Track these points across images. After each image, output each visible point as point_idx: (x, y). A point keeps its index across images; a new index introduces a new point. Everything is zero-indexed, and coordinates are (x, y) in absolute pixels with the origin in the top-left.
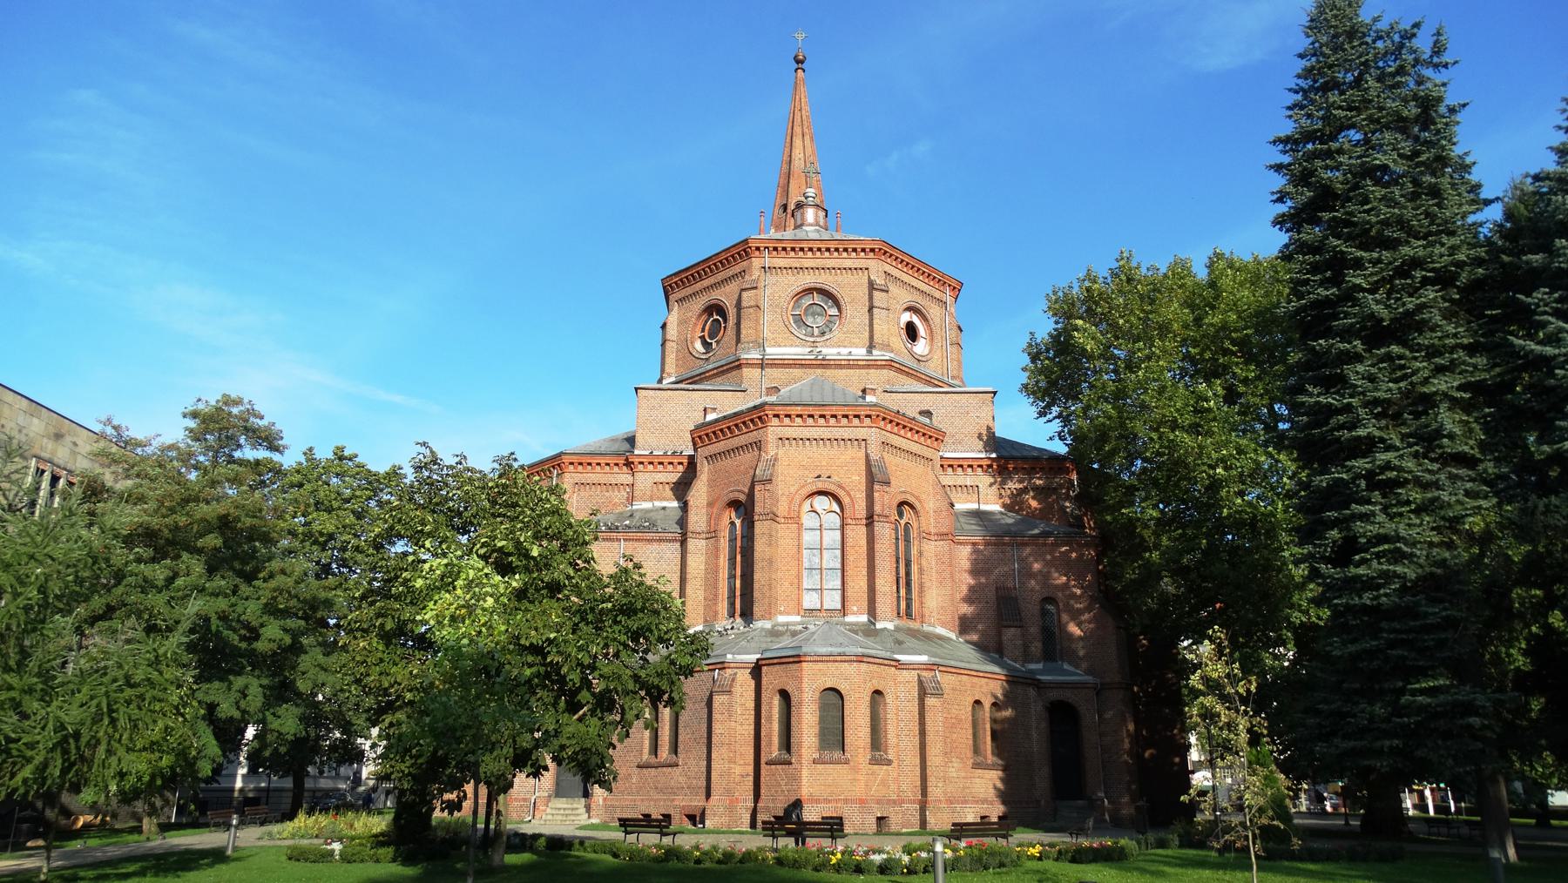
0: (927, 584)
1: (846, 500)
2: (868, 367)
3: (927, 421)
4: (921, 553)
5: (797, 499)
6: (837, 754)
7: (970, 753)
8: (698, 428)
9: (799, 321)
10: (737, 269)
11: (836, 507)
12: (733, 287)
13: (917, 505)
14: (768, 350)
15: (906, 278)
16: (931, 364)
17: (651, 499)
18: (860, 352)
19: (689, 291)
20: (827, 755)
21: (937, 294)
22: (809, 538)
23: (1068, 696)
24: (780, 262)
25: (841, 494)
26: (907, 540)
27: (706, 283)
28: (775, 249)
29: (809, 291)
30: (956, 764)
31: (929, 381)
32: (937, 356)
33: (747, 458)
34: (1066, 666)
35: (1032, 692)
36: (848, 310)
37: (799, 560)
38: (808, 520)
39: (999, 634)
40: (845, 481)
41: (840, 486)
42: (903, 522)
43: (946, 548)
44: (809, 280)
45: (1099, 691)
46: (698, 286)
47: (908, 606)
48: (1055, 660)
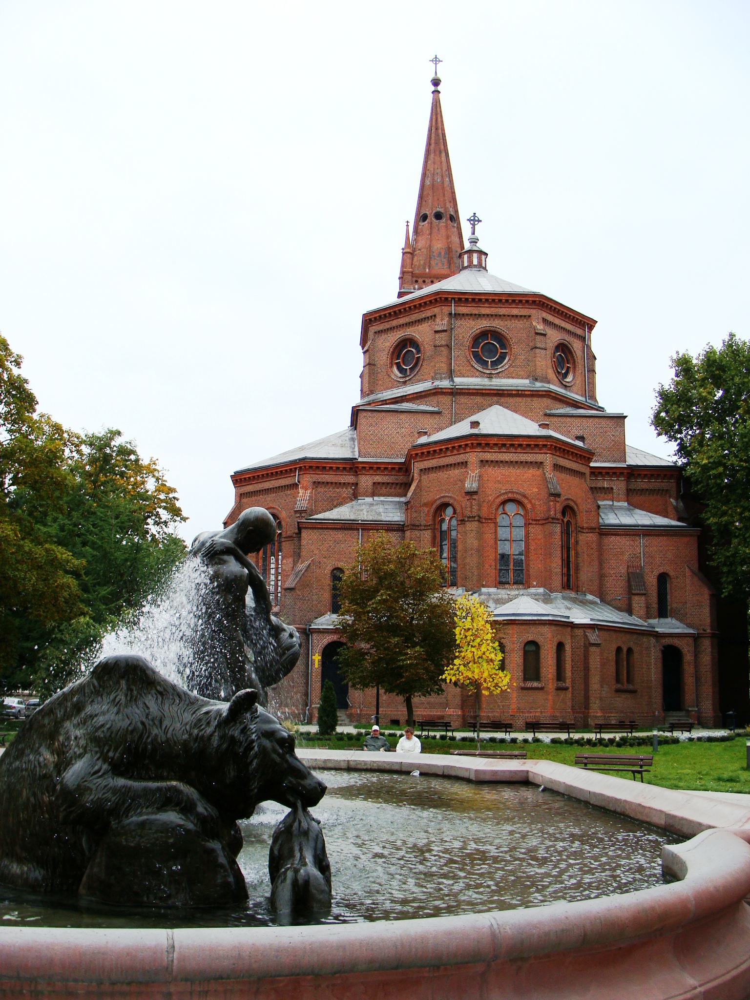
0: (581, 564)
1: (529, 506)
2: (532, 396)
3: (579, 443)
4: (577, 542)
5: (494, 507)
6: (535, 684)
7: (614, 682)
8: (415, 447)
9: (476, 356)
10: (429, 313)
11: (521, 512)
12: (425, 327)
13: (575, 507)
14: (456, 379)
15: (557, 321)
16: (574, 388)
17: (373, 495)
18: (523, 383)
19: (386, 326)
20: (529, 684)
21: (579, 332)
22: (503, 533)
23: (676, 642)
24: (463, 310)
25: (526, 501)
26: (568, 534)
27: (402, 321)
28: (460, 299)
29: (483, 334)
30: (606, 688)
31: (576, 405)
32: (579, 381)
33: (456, 472)
34: (674, 621)
35: (653, 640)
36: (516, 349)
37: (496, 549)
38: (502, 520)
39: (630, 599)
40: (528, 492)
41: (524, 496)
42: (565, 520)
43: (595, 539)
44: (484, 324)
45: (696, 638)
46: (395, 323)
47: (568, 580)
48: (666, 617)
